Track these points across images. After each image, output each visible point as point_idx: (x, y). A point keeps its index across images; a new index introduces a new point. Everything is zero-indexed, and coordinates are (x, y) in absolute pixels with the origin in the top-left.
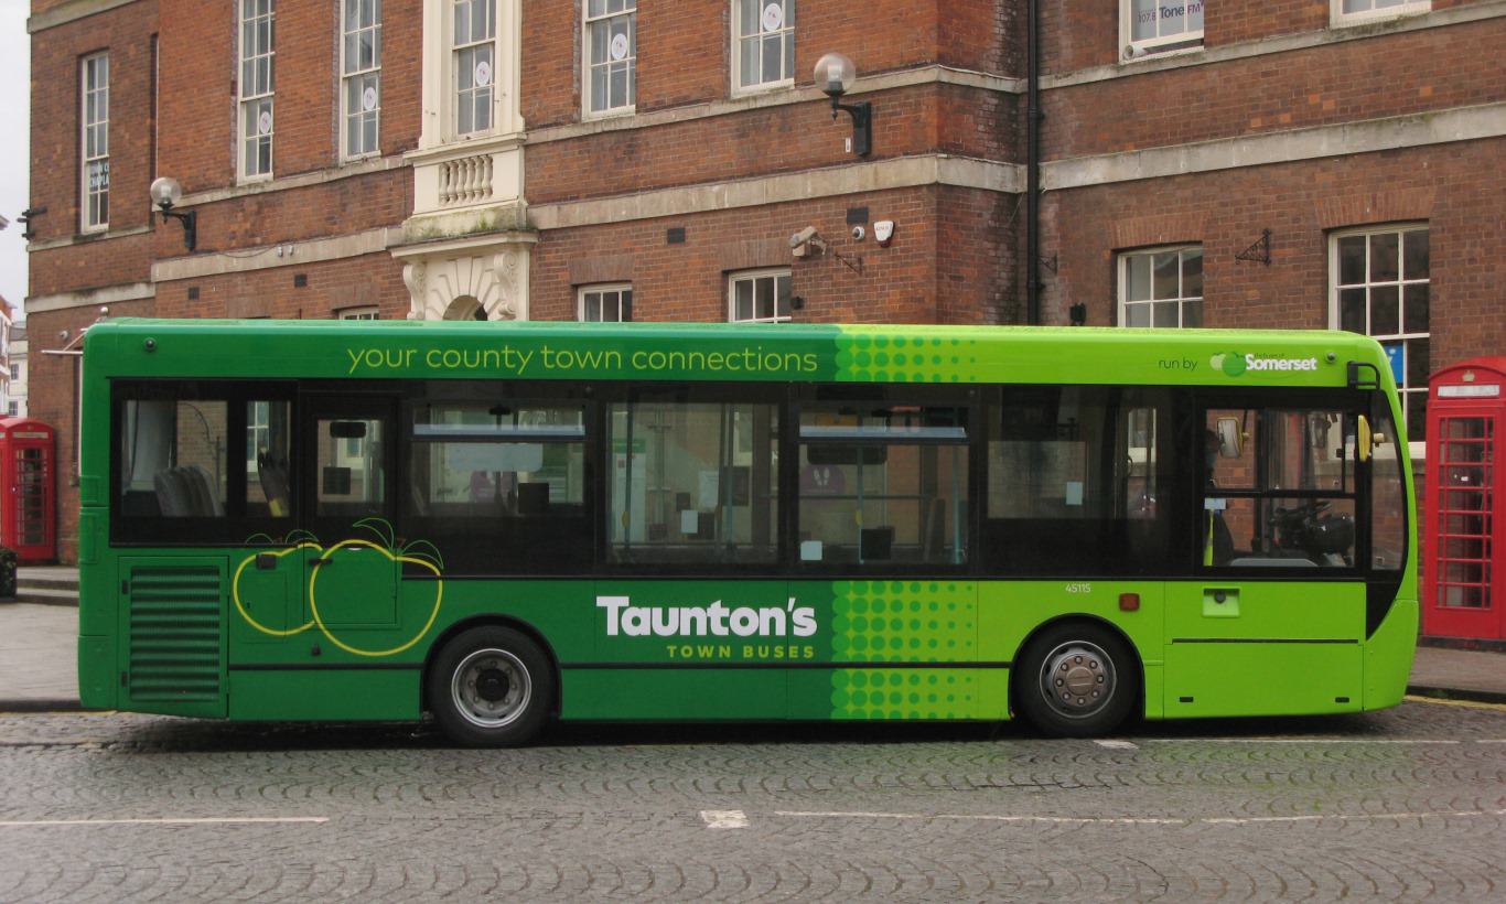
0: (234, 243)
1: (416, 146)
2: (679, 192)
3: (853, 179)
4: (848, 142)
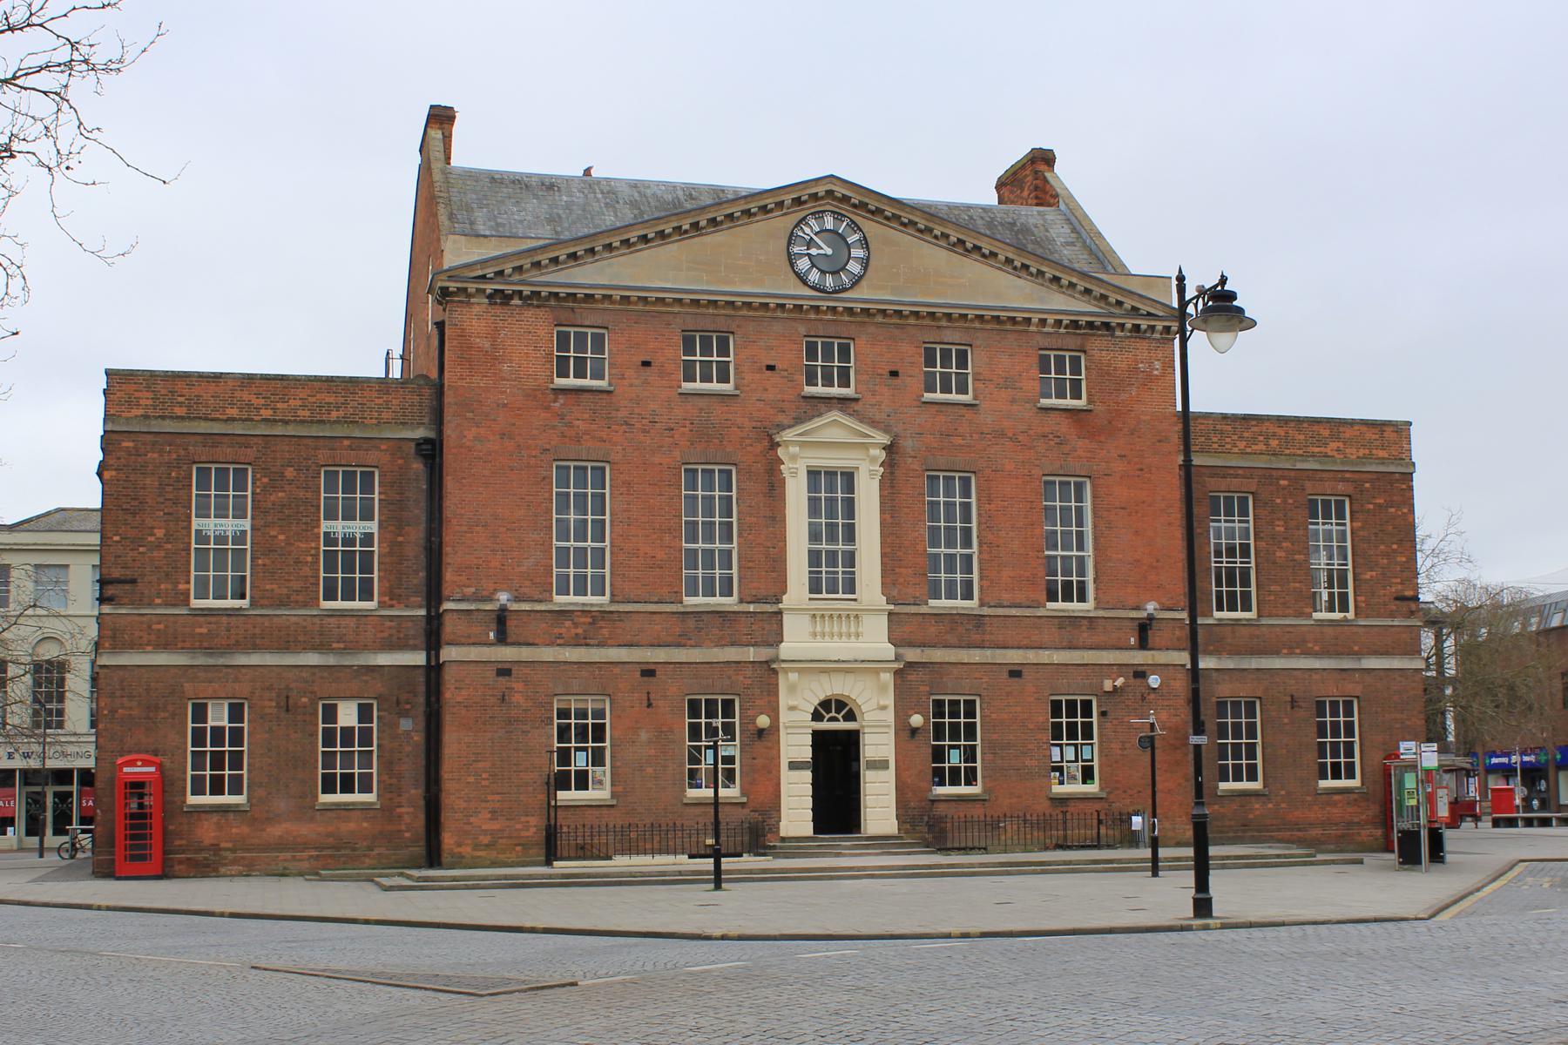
1: (779, 601)
2: (1021, 652)
4: (1132, 639)
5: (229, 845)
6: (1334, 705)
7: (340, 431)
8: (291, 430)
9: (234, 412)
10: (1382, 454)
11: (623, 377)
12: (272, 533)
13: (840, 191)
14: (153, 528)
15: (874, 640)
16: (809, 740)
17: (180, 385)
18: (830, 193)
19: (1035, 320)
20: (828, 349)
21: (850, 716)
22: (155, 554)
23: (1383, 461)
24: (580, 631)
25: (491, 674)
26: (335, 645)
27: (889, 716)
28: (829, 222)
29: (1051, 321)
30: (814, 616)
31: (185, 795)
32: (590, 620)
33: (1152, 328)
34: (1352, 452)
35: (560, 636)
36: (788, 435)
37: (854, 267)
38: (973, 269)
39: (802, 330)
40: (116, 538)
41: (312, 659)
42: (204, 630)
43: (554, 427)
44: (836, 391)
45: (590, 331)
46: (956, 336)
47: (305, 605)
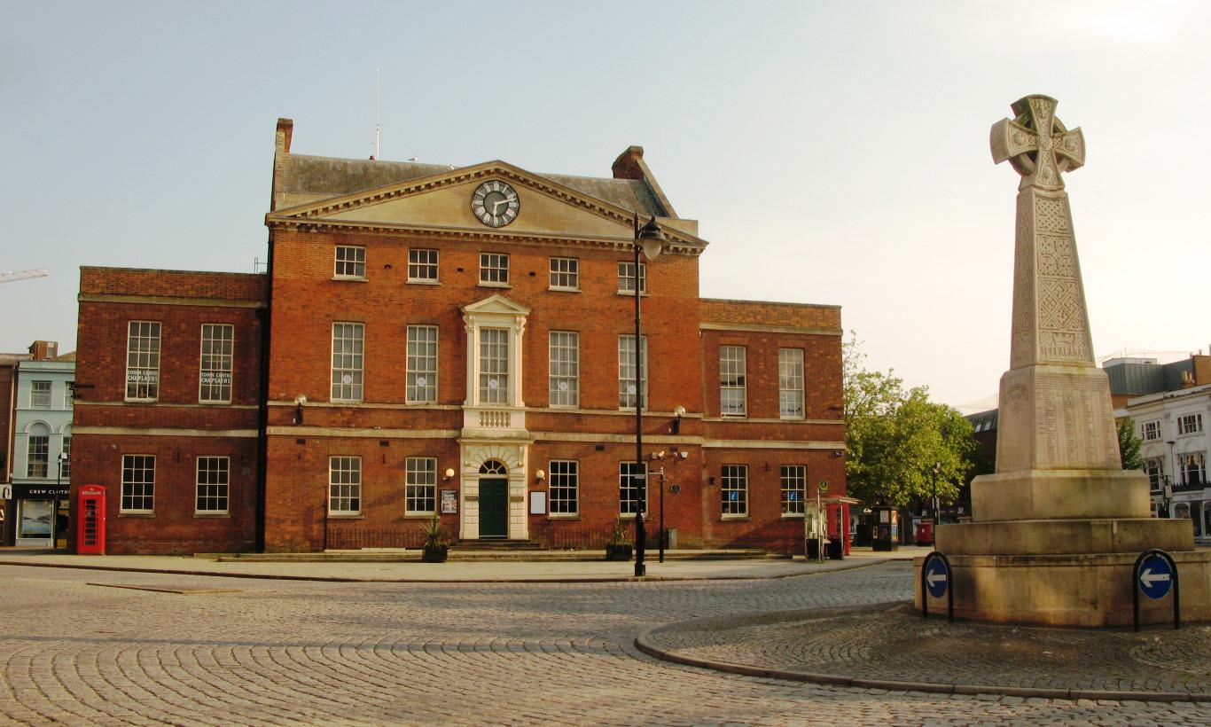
0: (333, 425)
1: (461, 403)
3: (673, 440)
5: (143, 537)
6: (792, 470)
7: (211, 303)
8: (185, 302)
9: (152, 291)
10: (824, 324)
11: (374, 274)
12: (173, 360)
13: (503, 169)
14: (104, 356)
15: (518, 424)
16: (477, 484)
17: (122, 275)
18: (497, 170)
19: (616, 245)
20: (494, 259)
21: (503, 471)
22: (105, 371)
23: (823, 329)
24: (345, 419)
25: (293, 442)
26: (207, 425)
27: (525, 471)
28: (497, 187)
29: (625, 245)
30: (482, 413)
31: (119, 508)
32: (351, 413)
33: (686, 250)
34: (806, 324)
35: (334, 422)
36: (468, 308)
37: (511, 213)
38: (581, 215)
39: (479, 248)
40: (84, 362)
41: (194, 433)
42: (132, 415)
43: (333, 302)
44: (498, 284)
45: (356, 248)
46: (570, 253)
47: (190, 402)
